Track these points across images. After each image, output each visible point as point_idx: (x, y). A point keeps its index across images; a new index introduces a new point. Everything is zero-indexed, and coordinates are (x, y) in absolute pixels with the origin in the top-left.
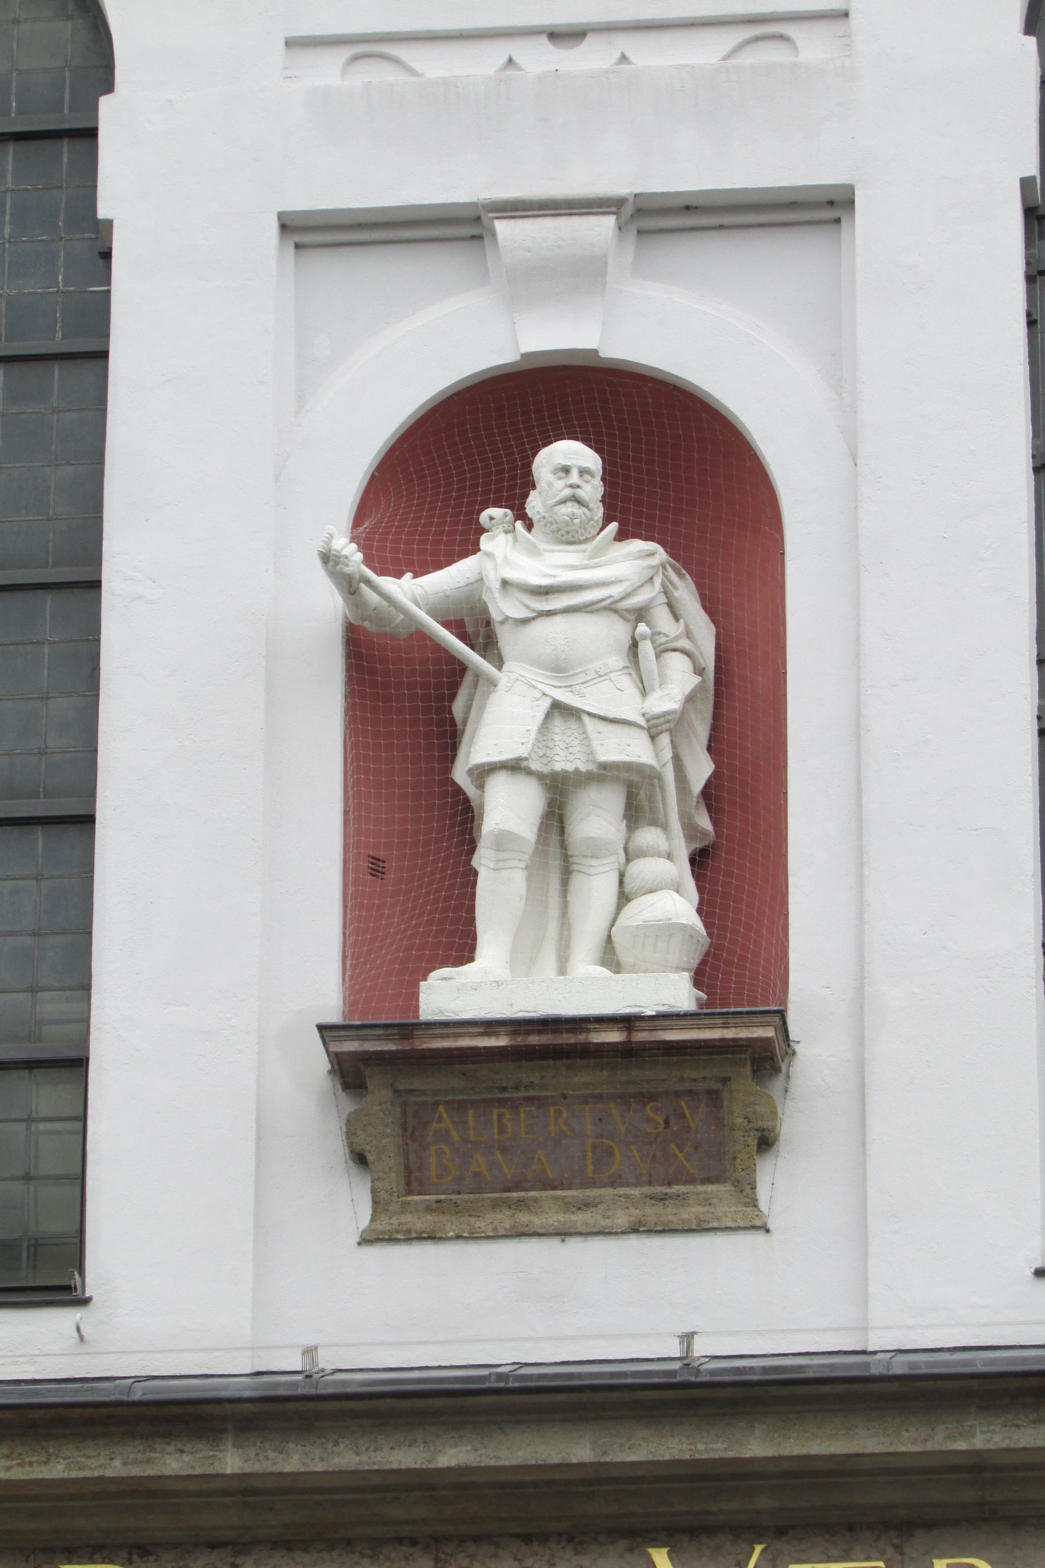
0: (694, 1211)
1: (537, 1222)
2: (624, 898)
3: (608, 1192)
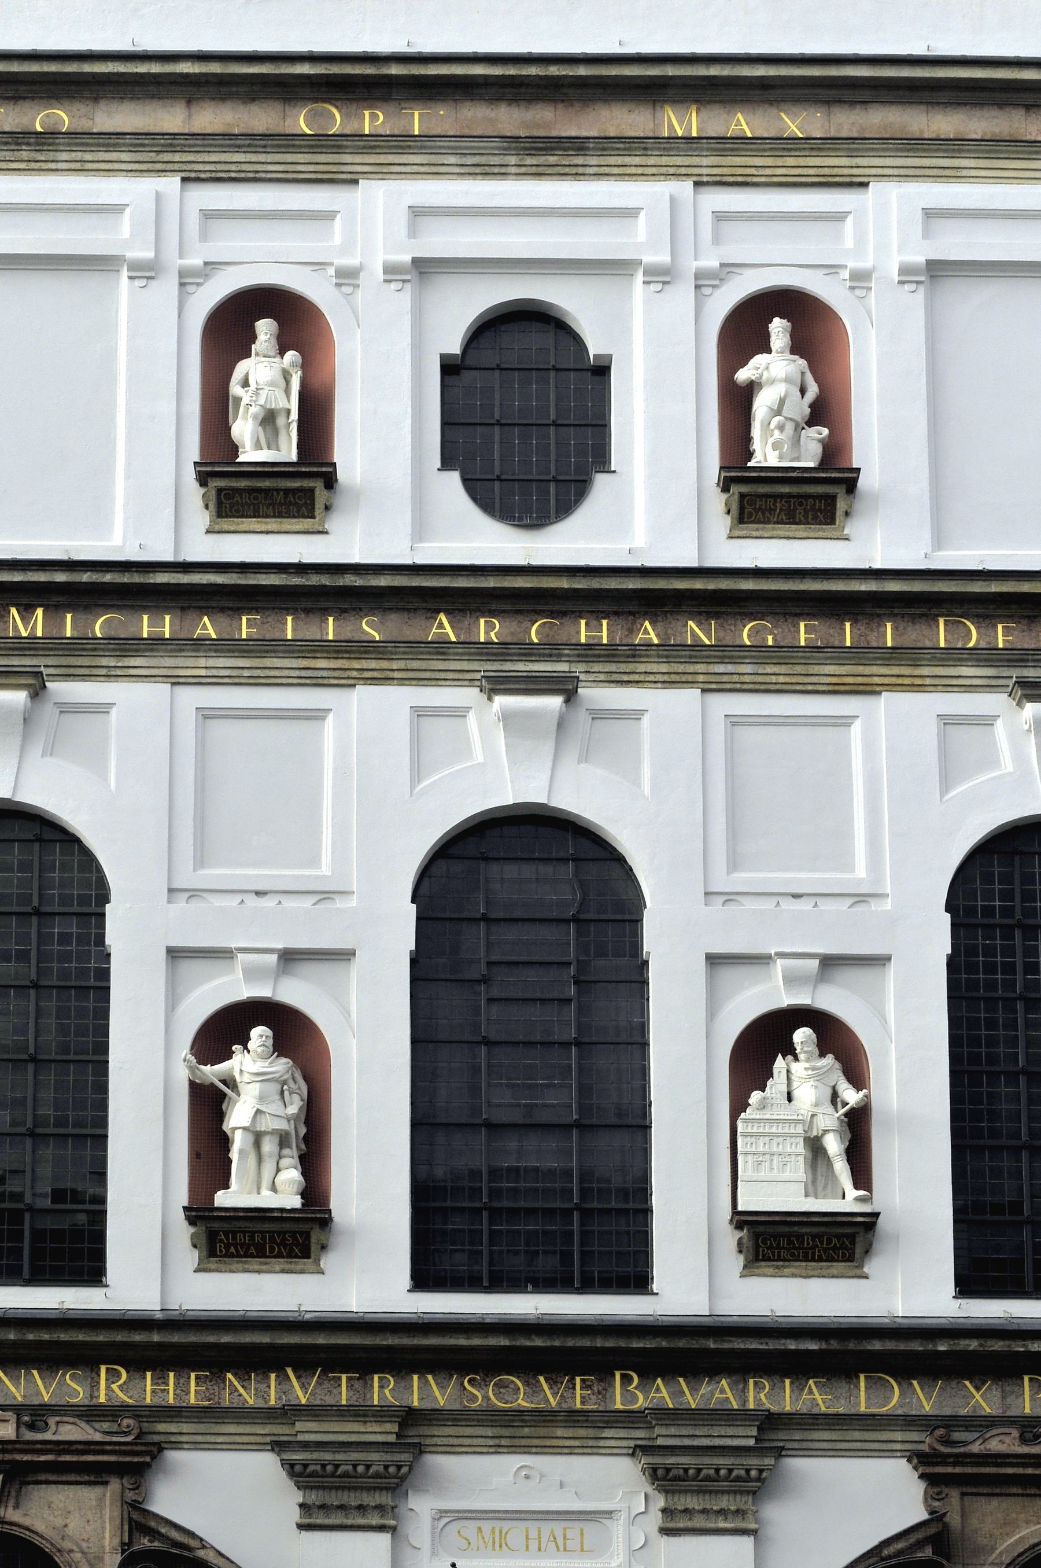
0: (299, 1267)
1: (251, 1268)
2: (278, 1170)
3: (273, 1260)
